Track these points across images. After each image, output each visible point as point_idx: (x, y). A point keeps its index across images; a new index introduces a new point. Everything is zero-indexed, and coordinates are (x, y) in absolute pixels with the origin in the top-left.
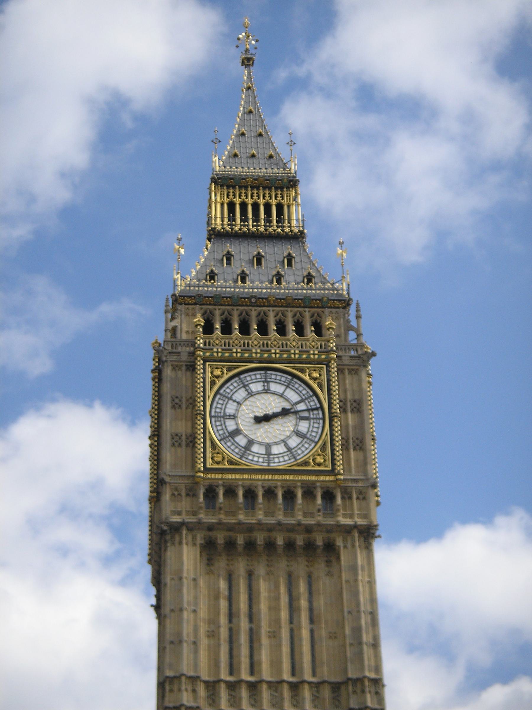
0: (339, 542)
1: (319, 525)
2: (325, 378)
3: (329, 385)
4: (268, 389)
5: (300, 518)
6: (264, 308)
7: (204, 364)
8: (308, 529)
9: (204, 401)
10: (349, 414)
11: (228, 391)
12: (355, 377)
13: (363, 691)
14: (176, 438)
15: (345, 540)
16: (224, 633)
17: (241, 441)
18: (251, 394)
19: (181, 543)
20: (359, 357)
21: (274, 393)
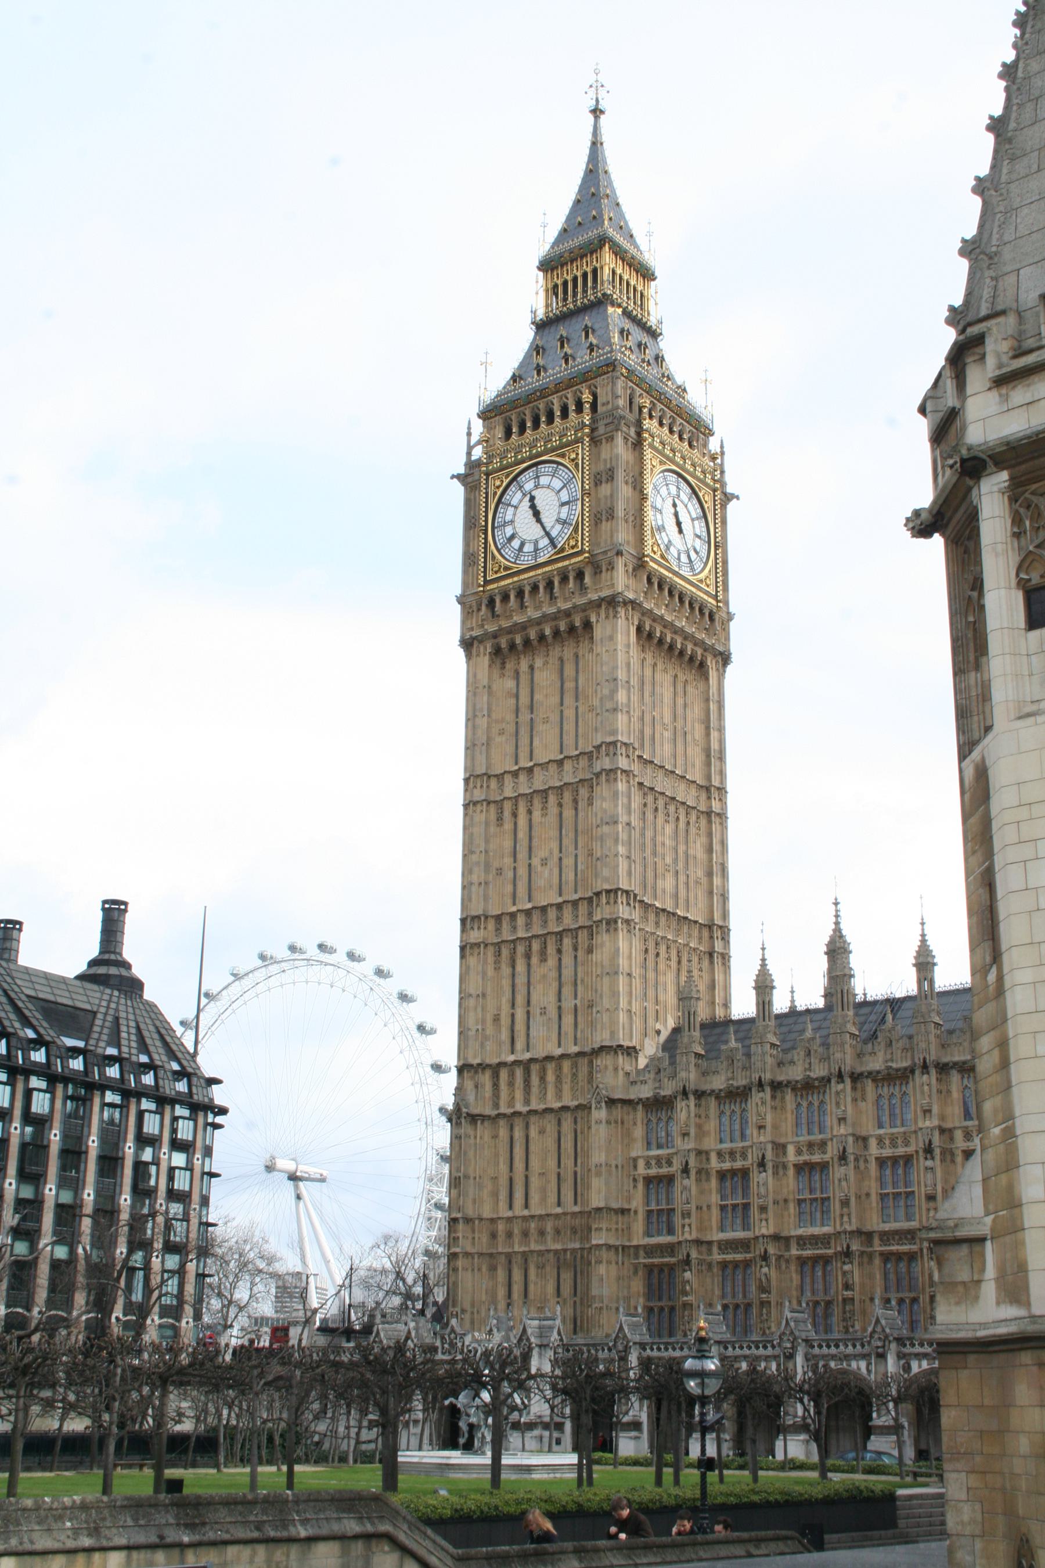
1: (574, 607)
2: (580, 456)
3: (583, 463)
7: (487, 480)
8: (568, 614)
9: (486, 516)
10: (604, 485)
16: (512, 728)
17: (516, 543)
18: (524, 495)
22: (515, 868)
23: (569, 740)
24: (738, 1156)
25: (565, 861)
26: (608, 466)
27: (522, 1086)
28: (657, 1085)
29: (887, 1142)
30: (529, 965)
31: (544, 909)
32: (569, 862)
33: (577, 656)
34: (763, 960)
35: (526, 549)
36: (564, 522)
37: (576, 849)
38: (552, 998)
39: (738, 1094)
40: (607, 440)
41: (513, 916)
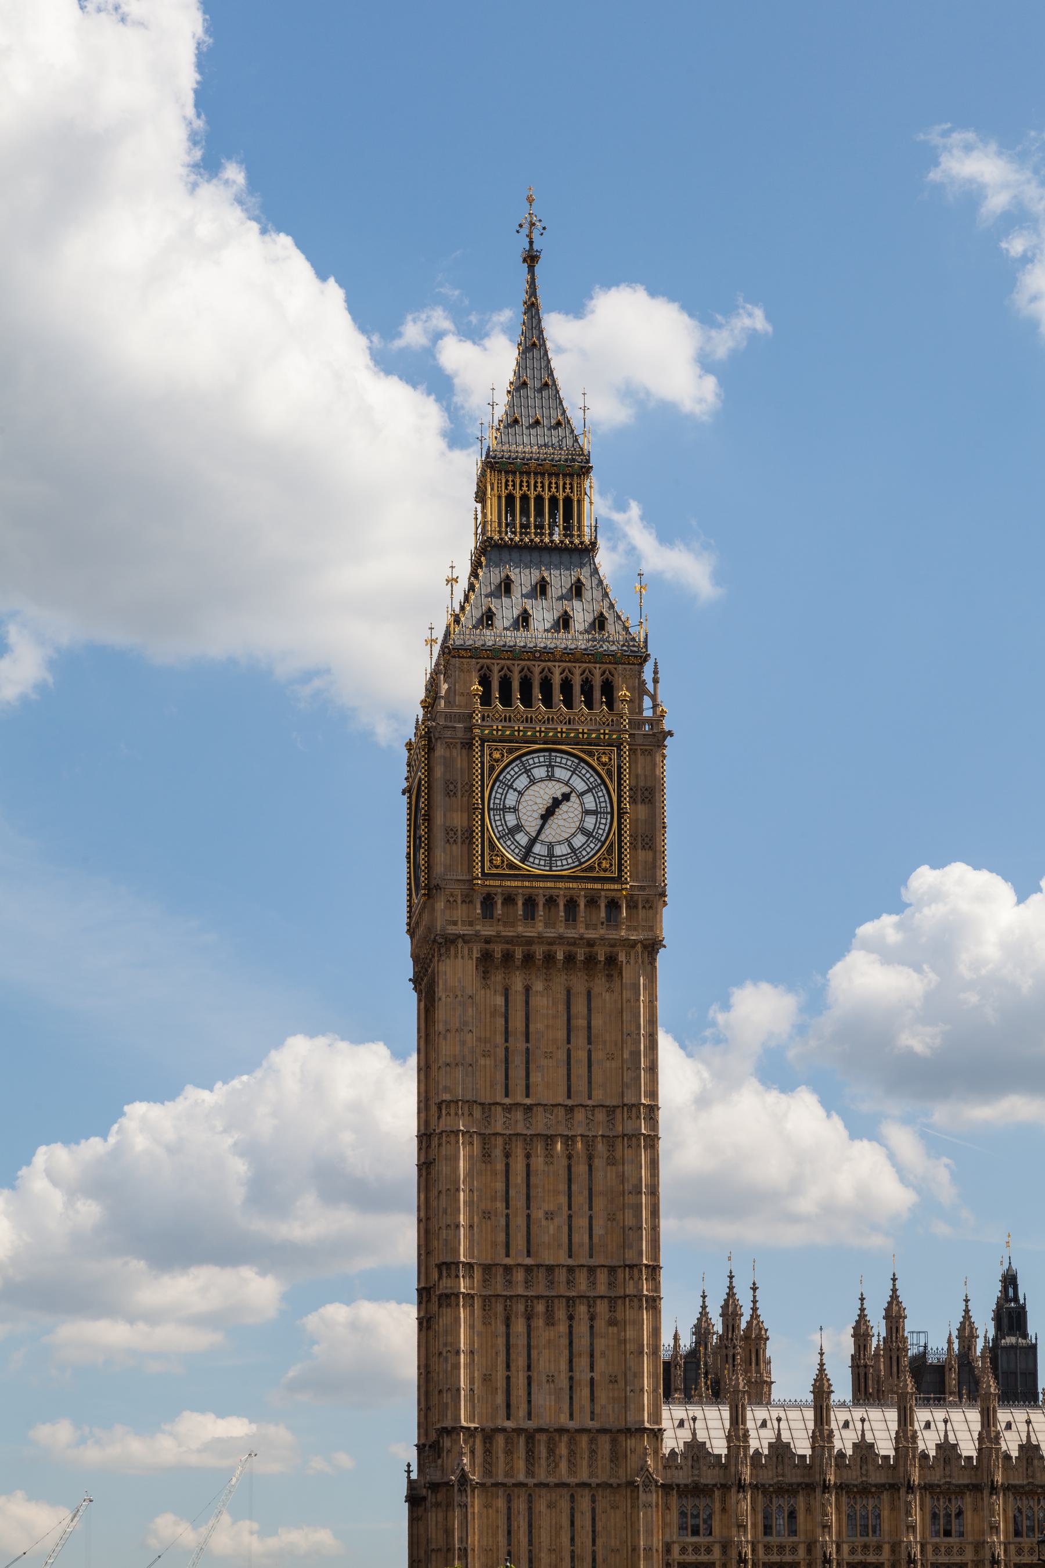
0: (622, 957)
2: (615, 762)
3: (620, 773)
4: (553, 776)
5: (582, 931)
6: (549, 664)
7: (482, 745)
8: (591, 943)
10: (639, 806)
11: (509, 777)
12: (649, 758)
13: (638, 1117)
14: (451, 834)
15: (628, 955)
16: (500, 1053)
18: (533, 782)
19: (456, 957)
20: (654, 735)
21: (558, 781)
22: (507, 1216)
23: (580, 1084)
24: (788, 1549)
25: (575, 1222)
26: (642, 784)
27: (524, 1457)
28: (696, 1472)
29: (943, 1550)
30: (529, 1326)
31: (550, 1269)
32: (584, 1222)
33: (589, 993)
34: (822, 1365)
35: (538, 849)
36: (588, 834)
37: (591, 1208)
38: (564, 1366)
39: (788, 1491)
40: (643, 752)
41: (508, 1269)
